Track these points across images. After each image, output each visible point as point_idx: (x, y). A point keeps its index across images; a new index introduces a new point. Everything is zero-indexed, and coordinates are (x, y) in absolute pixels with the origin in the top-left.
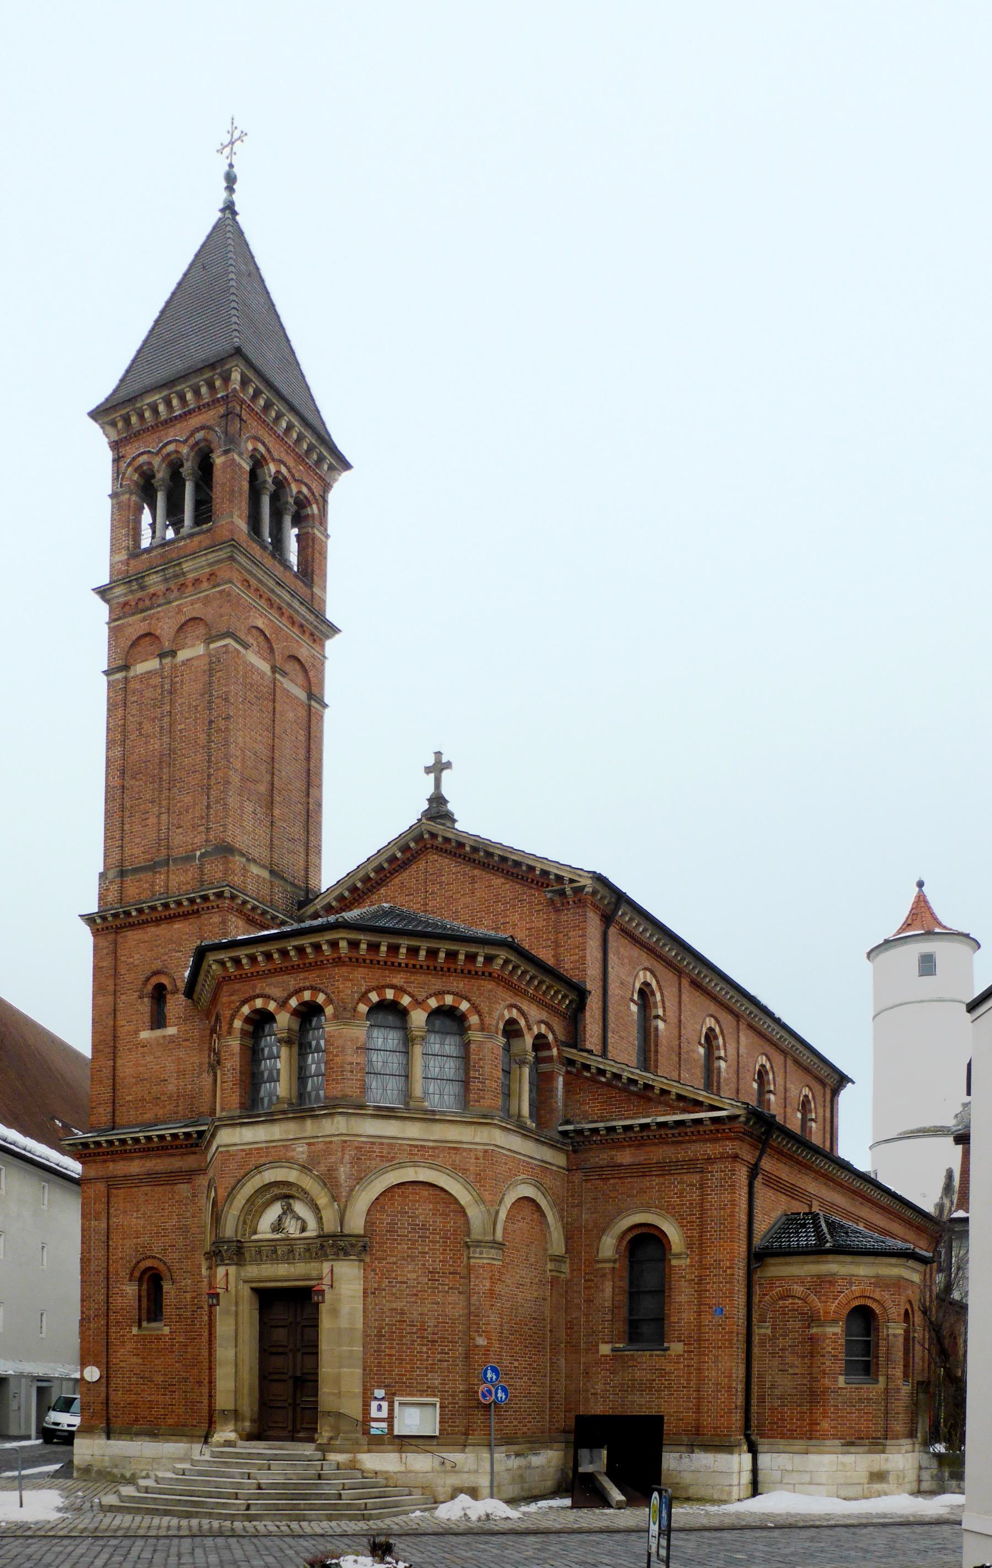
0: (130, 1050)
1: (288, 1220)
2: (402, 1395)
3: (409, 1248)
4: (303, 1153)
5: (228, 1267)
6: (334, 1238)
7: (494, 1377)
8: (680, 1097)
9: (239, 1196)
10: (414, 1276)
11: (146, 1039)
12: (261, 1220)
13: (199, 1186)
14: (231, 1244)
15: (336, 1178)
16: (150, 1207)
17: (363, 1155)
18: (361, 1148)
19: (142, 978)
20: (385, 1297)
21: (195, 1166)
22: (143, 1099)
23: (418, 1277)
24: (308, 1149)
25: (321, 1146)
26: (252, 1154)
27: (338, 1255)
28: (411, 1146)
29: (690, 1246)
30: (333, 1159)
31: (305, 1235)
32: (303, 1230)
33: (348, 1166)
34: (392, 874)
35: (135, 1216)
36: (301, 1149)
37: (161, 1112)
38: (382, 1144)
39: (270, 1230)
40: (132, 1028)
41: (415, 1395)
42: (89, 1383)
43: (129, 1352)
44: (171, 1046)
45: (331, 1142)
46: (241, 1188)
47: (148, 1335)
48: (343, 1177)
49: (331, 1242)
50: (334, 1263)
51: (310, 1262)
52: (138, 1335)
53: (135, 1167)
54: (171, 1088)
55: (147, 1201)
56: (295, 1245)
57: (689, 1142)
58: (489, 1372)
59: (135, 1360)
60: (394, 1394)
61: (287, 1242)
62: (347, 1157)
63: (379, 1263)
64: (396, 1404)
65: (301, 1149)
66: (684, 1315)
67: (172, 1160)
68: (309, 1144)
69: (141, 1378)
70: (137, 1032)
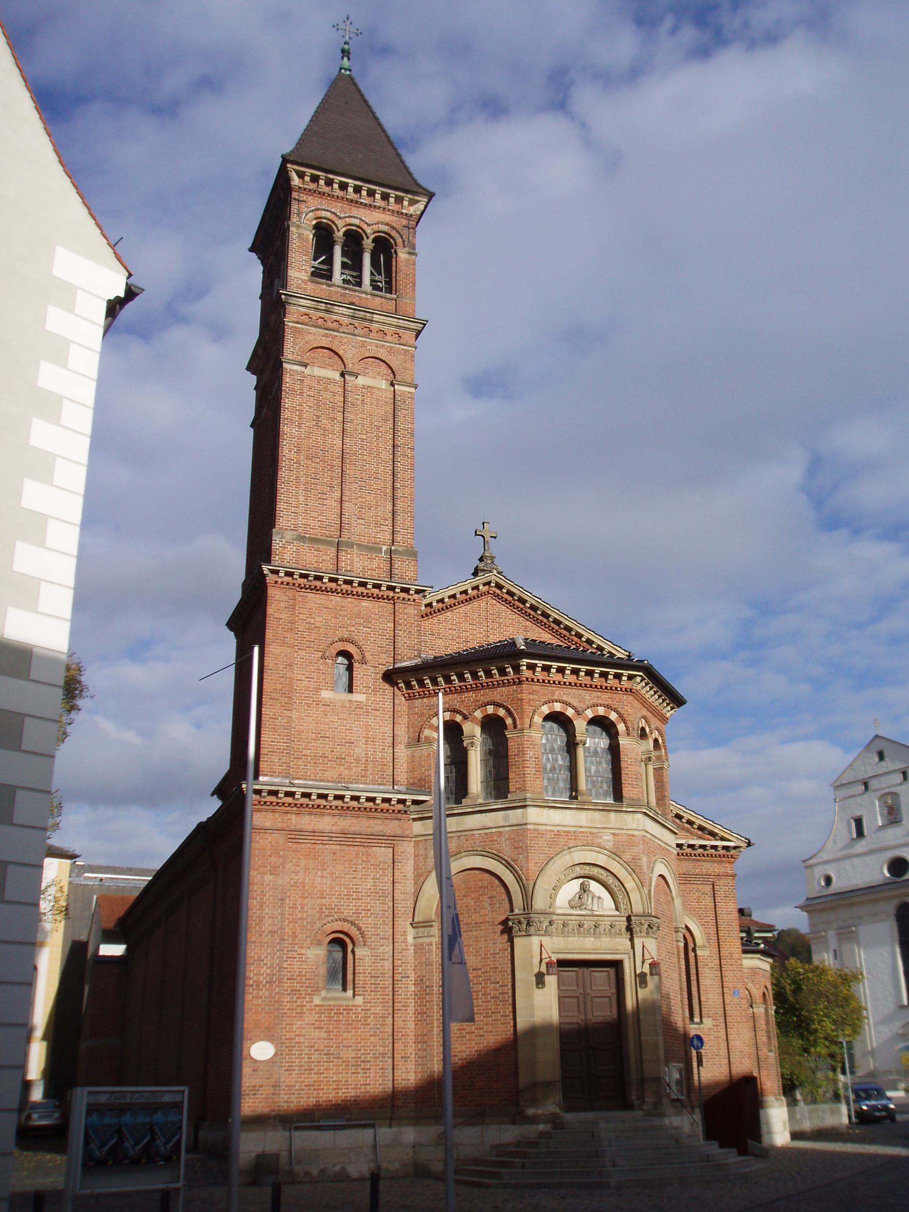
0: (309, 705)
1: (590, 898)
4: (609, 841)
5: (542, 938)
7: (700, 1045)
8: (701, 828)
11: (329, 699)
13: (402, 852)
16: (340, 868)
19: (329, 641)
21: (399, 832)
22: (324, 756)
25: (625, 837)
26: (561, 835)
29: (708, 940)
34: (459, 604)
35: (319, 873)
36: (607, 838)
37: (346, 772)
40: (313, 685)
42: (255, 1061)
43: (308, 1024)
44: (358, 711)
45: (633, 836)
47: (335, 1006)
52: (321, 1006)
53: (325, 823)
54: (359, 750)
55: (334, 860)
57: (704, 861)
58: (695, 1040)
59: (316, 1034)
65: (607, 838)
66: (710, 996)
67: (372, 822)
68: (614, 834)
69: (325, 1054)
70: (318, 690)
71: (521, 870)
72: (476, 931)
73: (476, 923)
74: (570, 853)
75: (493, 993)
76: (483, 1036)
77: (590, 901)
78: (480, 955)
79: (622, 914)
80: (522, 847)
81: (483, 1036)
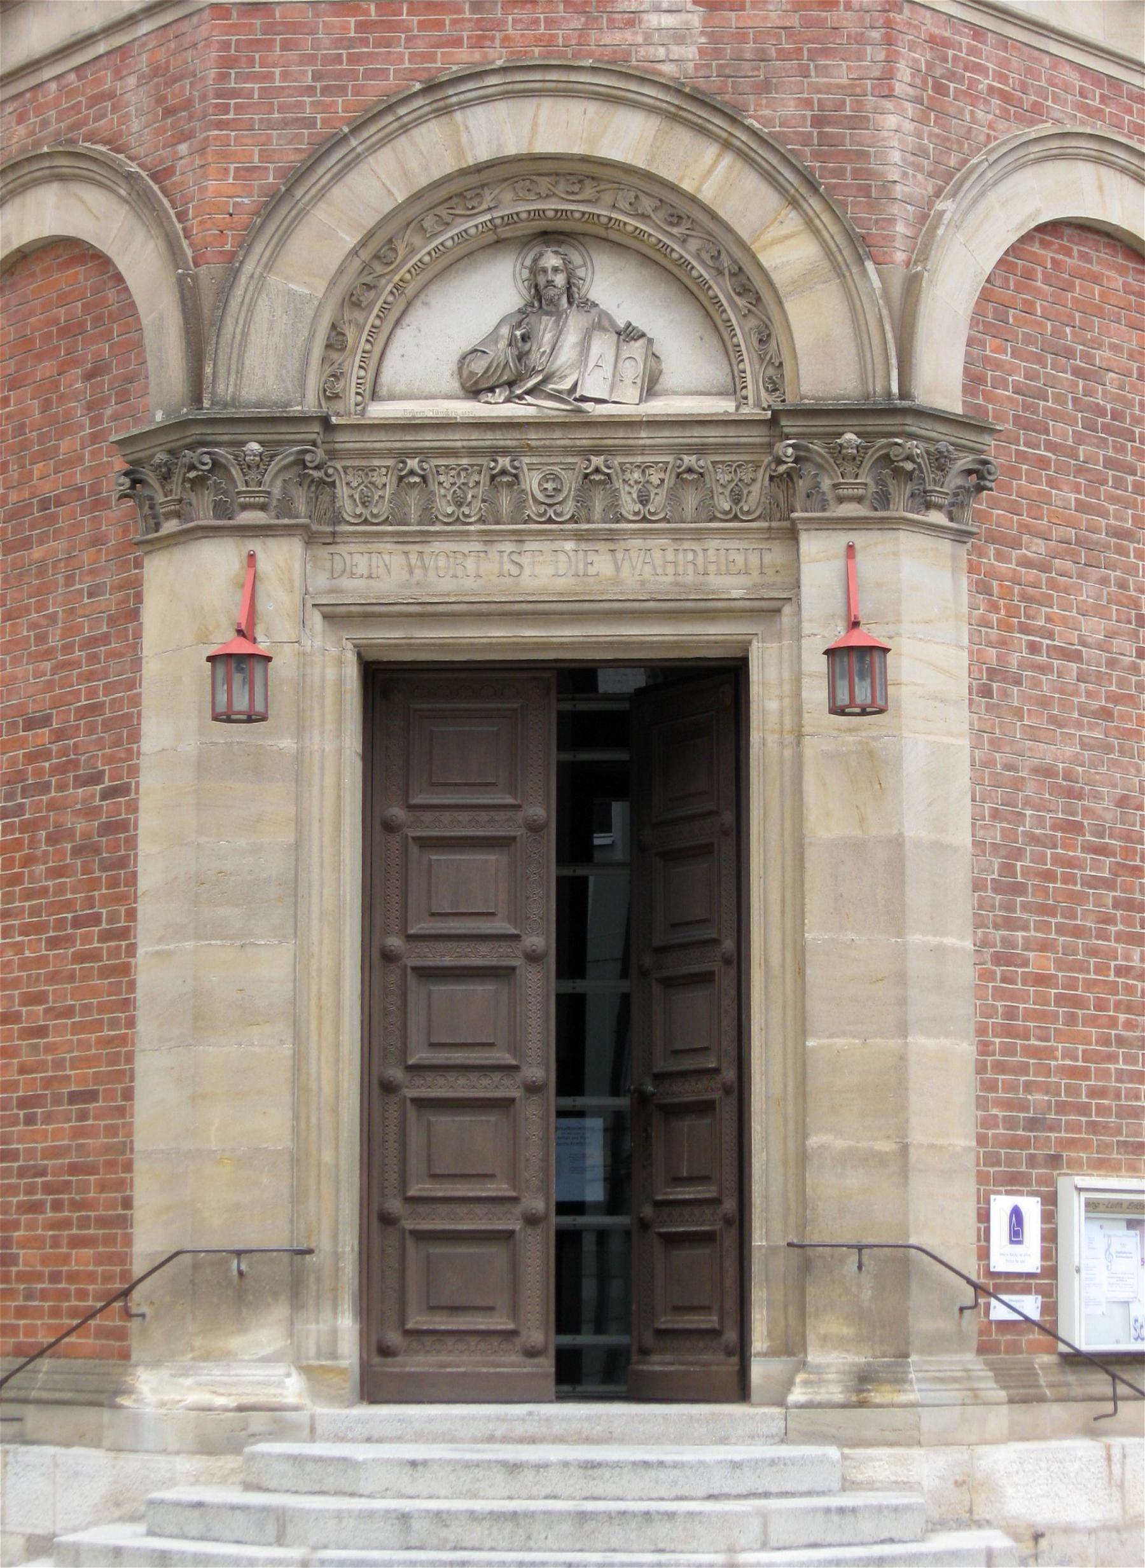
2: (1101, 1165)
3: (1081, 506)
4: (679, 37)
5: (255, 545)
6: (873, 424)
9: (321, 214)
10: (1094, 628)
12: (404, 337)
14: (285, 432)
15: (862, 155)
17: (952, 76)
18: (945, 43)
20: (1019, 713)
23: (1110, 635)
24: (705, 22)
27: (883, 499)
28: (1083, 70)
30: (841, 73)
31: (657, 407)
32: (651, 387)
33: (909, 106)
38: (1004, 42)
39: (454, 385)
41: (1113, 1168)
46: (337, 178)
48: (896, 156)
49: (850, 436)
50: (859, 538)
51: (699, 535)
56: (629, 450)
60: (1054, 1161)
61: (584, 438)
62: (904, 72)
63: (1000, 557)
64: (1073, 1208)
71: (182, 216)
72: (41, 542)
73: (44, 505)
74: (446, 111)
75: (80, 825)
76: (42, 1032)
77: (567, 353)
78: (48, 654)
79: (749, 412)
80: (188, 104)
81: (42, 1032)
